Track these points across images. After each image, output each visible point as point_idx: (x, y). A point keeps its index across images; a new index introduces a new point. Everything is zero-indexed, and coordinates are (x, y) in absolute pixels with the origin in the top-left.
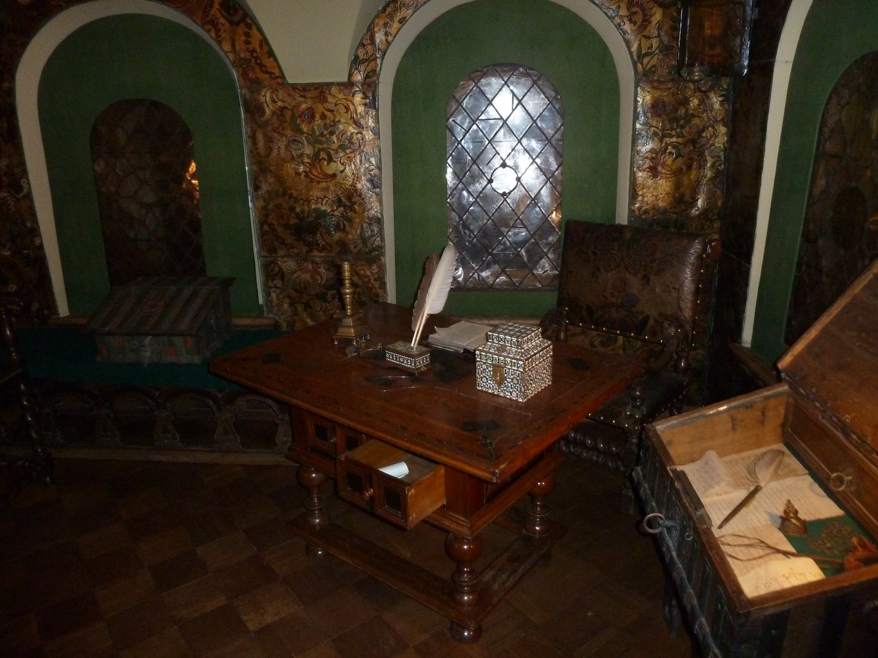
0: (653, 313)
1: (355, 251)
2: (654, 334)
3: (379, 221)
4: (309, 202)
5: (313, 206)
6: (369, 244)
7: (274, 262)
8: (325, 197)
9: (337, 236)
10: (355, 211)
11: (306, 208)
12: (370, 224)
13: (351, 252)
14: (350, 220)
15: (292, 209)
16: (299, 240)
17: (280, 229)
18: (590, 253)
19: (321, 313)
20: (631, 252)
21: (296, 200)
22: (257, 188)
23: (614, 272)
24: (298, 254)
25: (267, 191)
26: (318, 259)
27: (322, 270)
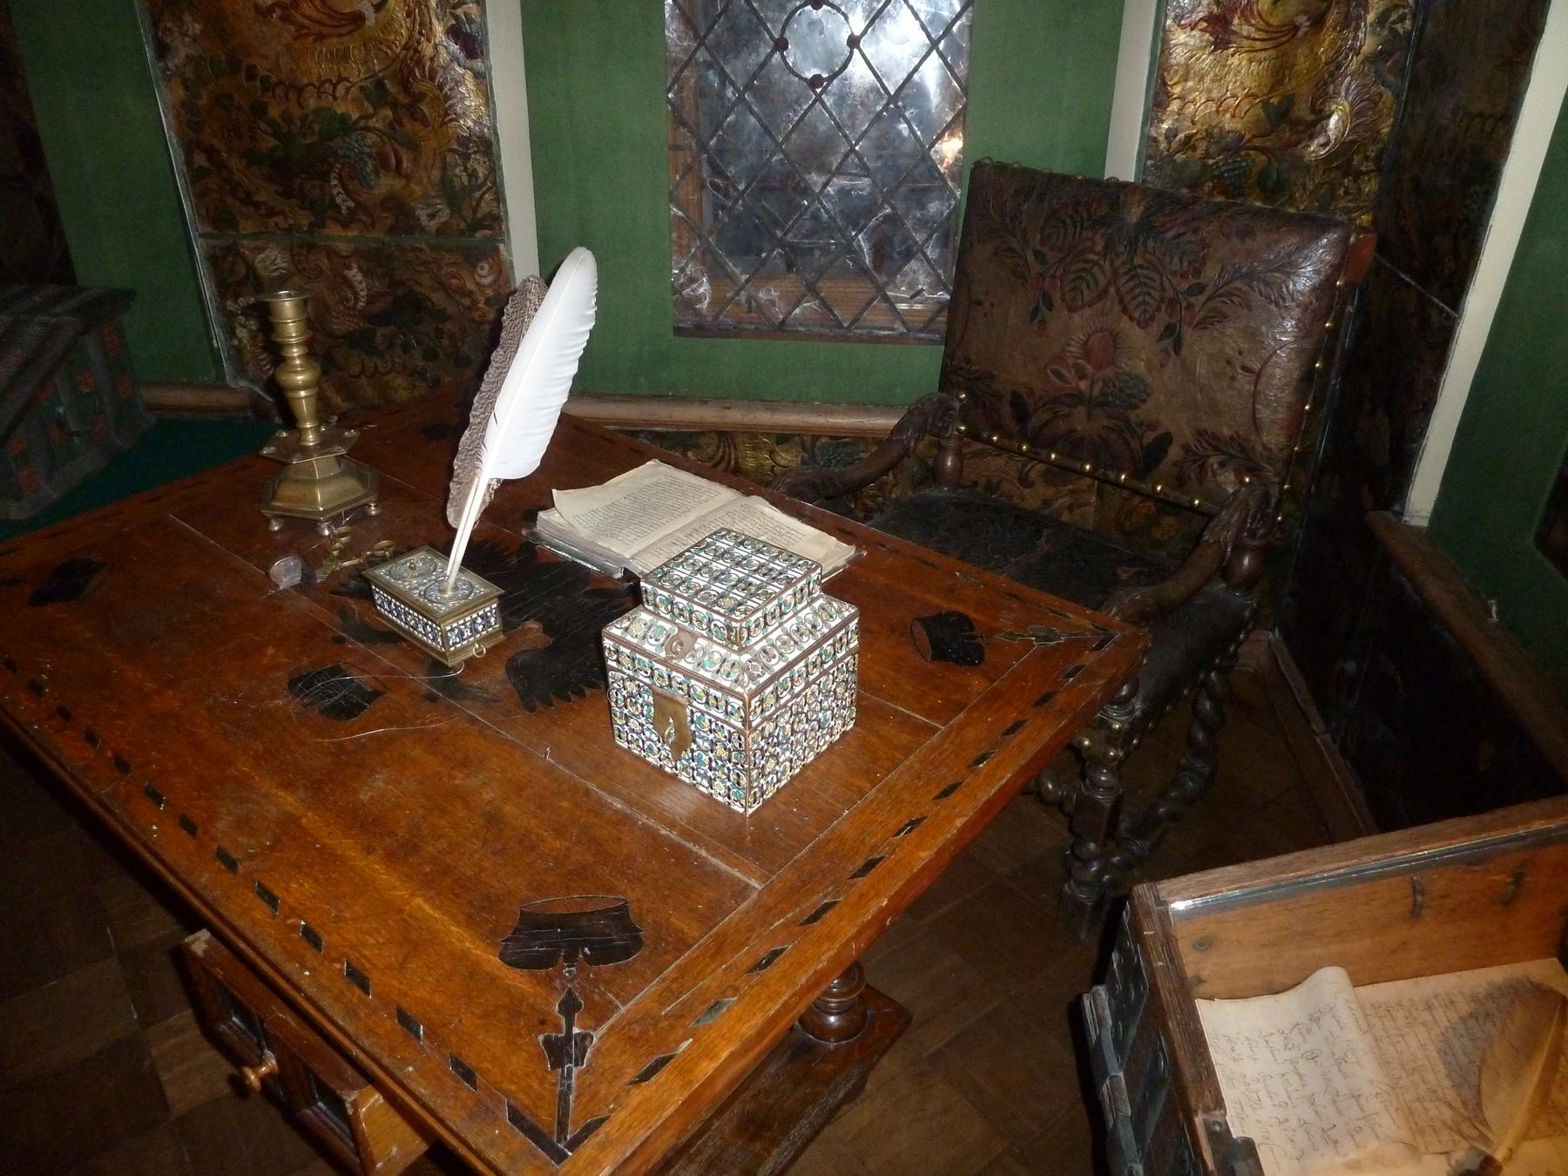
0: (1181, 426)
1: (433, 225)
2: (1180, 482)
3: (487, 146)
4: (300, 90)
5: (312, 103)
6: (468, 213)
7: (232, 250)
8: (341, 79)
9: (385, 184)
10: (424, 122)
11: (297, 112)
12: (466, 157)
13: (423, 229)
14: (413, 146)
15: (259, 110)
16: (287, 194)
17: (235, 163)
18: (1031, 258)
19: (364, 380)
20: (1138, 261)
21: (268, 87)
22: (162, 50)
23: (1087, 312)
24: (290, 230)
25: (189, 58)
26: (343, 248)
27: (355, 274)
